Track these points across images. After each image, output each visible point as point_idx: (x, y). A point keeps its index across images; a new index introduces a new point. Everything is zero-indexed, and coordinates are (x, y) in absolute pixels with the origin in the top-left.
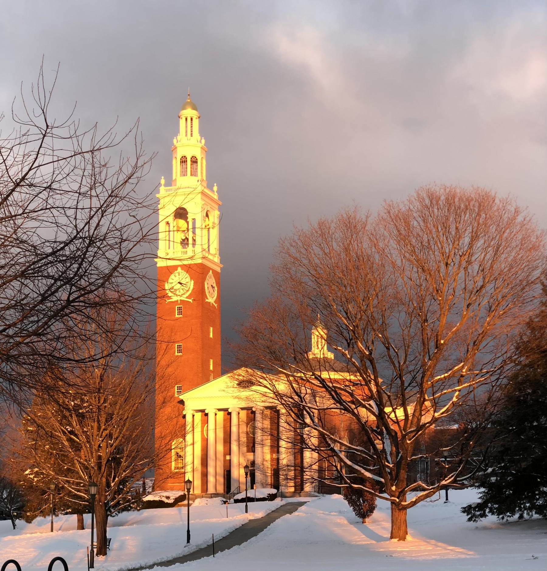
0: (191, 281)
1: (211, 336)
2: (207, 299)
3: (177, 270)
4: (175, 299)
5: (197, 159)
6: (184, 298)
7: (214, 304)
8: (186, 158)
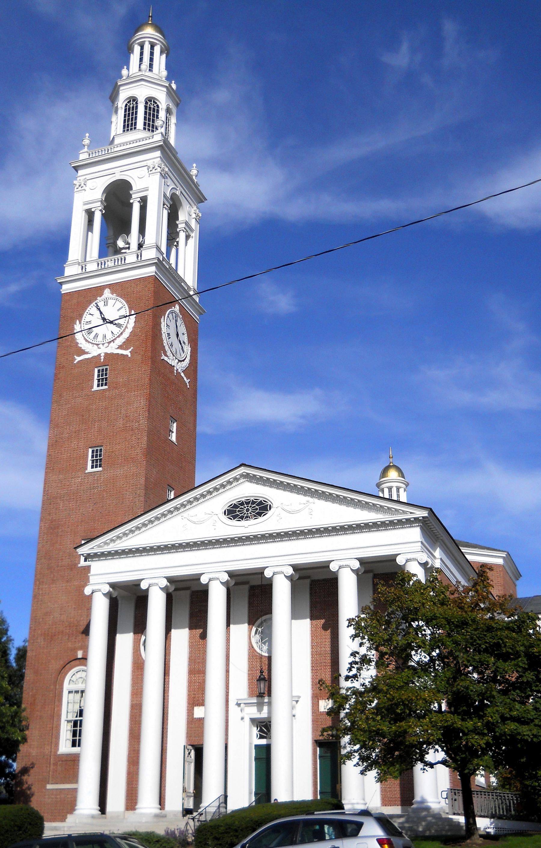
1: (173, 437)
4: (93, 351)
5: (158, 106)
6: (113, 349)
7: (182, 374)
8: (137, 103)
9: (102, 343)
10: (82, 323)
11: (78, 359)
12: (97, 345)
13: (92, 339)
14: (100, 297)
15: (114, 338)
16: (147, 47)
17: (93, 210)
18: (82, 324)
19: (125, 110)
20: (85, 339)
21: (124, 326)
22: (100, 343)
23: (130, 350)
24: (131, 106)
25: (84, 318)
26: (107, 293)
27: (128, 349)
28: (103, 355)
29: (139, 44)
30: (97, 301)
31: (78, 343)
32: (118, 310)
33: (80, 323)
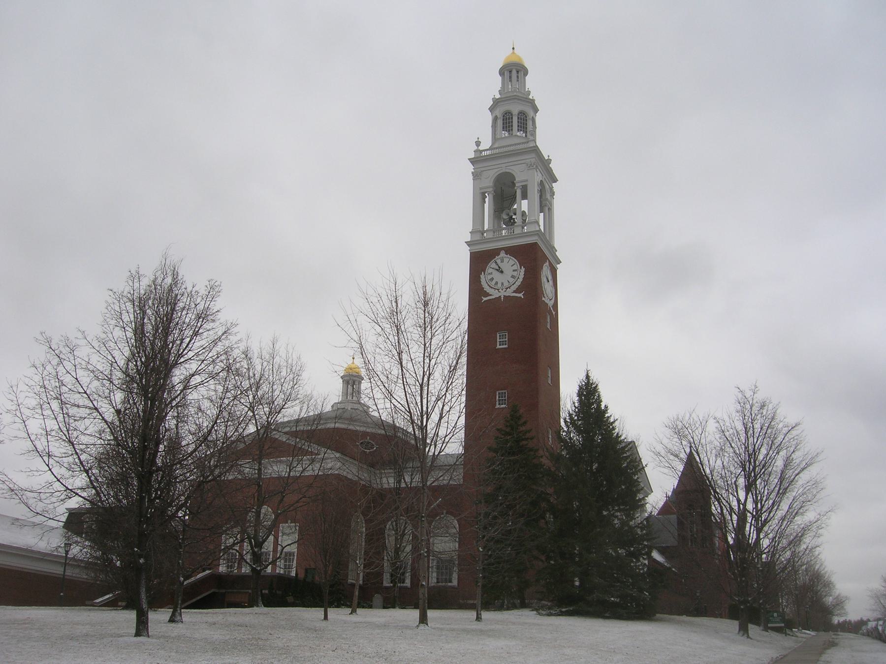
2: (544, 297)
3: (498, 254)
4: (495, 294)
6: (509, 293)
8: (512, 115)
12: (498, 290)
14: (498, 256)
16: (514, 72)
19: (503, 120)
20: (488, 285)
21: (517, 277)
24: (508, 117)
25: (487, 270)
26: (502, 254)
27: (520, 293)
28: (502, 296)
30: (495, 259)
31: (484, 288)
32: (512, 266)
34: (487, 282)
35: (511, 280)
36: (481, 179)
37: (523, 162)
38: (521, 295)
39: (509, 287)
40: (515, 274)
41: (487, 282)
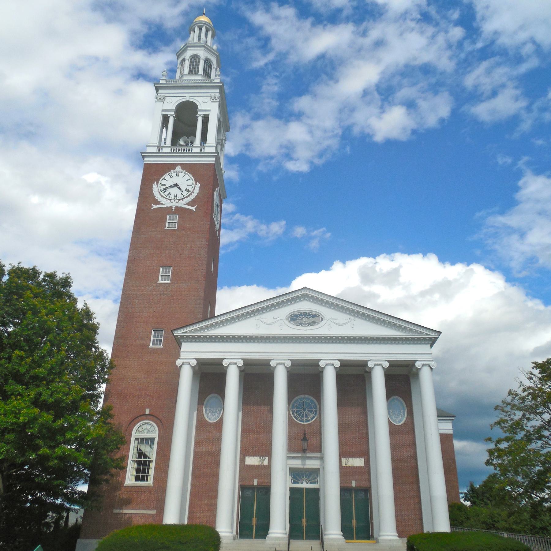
0: (196, 184)
3: (174, 169)
4: (166, 204)
6: (182, 204)
8: (199, 59)
9: (174, 199)
10: (159, 184)
11: (155, 207)
13: (166, 196)
14: (173, 170)
15: (183, 197)
16: (204, 30)
17: (169, 115)
18: (159, 185)
21: (191, 191)
22: (172, 199)
23: (195, 207)
24: (195, 60)
25: (160, 181)
26: (178, 168)
28: (174, 207)
29: (198, 27)
30: (170, 172)
32: (187, 180)
33: (157, 184)
34: (159, 192)
35: (185, 193)
36: (163, 103)
37: (209, 94)
38: (193, 208)
39: (182, 199)
40: (189, 188)
41: (159, 192)
